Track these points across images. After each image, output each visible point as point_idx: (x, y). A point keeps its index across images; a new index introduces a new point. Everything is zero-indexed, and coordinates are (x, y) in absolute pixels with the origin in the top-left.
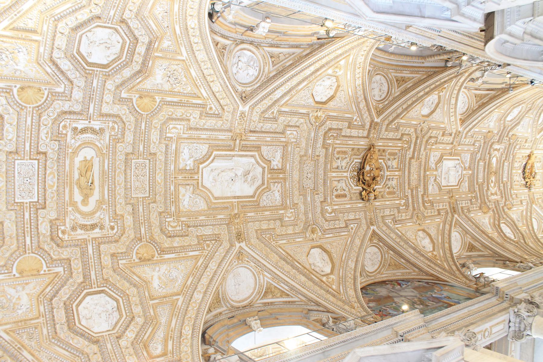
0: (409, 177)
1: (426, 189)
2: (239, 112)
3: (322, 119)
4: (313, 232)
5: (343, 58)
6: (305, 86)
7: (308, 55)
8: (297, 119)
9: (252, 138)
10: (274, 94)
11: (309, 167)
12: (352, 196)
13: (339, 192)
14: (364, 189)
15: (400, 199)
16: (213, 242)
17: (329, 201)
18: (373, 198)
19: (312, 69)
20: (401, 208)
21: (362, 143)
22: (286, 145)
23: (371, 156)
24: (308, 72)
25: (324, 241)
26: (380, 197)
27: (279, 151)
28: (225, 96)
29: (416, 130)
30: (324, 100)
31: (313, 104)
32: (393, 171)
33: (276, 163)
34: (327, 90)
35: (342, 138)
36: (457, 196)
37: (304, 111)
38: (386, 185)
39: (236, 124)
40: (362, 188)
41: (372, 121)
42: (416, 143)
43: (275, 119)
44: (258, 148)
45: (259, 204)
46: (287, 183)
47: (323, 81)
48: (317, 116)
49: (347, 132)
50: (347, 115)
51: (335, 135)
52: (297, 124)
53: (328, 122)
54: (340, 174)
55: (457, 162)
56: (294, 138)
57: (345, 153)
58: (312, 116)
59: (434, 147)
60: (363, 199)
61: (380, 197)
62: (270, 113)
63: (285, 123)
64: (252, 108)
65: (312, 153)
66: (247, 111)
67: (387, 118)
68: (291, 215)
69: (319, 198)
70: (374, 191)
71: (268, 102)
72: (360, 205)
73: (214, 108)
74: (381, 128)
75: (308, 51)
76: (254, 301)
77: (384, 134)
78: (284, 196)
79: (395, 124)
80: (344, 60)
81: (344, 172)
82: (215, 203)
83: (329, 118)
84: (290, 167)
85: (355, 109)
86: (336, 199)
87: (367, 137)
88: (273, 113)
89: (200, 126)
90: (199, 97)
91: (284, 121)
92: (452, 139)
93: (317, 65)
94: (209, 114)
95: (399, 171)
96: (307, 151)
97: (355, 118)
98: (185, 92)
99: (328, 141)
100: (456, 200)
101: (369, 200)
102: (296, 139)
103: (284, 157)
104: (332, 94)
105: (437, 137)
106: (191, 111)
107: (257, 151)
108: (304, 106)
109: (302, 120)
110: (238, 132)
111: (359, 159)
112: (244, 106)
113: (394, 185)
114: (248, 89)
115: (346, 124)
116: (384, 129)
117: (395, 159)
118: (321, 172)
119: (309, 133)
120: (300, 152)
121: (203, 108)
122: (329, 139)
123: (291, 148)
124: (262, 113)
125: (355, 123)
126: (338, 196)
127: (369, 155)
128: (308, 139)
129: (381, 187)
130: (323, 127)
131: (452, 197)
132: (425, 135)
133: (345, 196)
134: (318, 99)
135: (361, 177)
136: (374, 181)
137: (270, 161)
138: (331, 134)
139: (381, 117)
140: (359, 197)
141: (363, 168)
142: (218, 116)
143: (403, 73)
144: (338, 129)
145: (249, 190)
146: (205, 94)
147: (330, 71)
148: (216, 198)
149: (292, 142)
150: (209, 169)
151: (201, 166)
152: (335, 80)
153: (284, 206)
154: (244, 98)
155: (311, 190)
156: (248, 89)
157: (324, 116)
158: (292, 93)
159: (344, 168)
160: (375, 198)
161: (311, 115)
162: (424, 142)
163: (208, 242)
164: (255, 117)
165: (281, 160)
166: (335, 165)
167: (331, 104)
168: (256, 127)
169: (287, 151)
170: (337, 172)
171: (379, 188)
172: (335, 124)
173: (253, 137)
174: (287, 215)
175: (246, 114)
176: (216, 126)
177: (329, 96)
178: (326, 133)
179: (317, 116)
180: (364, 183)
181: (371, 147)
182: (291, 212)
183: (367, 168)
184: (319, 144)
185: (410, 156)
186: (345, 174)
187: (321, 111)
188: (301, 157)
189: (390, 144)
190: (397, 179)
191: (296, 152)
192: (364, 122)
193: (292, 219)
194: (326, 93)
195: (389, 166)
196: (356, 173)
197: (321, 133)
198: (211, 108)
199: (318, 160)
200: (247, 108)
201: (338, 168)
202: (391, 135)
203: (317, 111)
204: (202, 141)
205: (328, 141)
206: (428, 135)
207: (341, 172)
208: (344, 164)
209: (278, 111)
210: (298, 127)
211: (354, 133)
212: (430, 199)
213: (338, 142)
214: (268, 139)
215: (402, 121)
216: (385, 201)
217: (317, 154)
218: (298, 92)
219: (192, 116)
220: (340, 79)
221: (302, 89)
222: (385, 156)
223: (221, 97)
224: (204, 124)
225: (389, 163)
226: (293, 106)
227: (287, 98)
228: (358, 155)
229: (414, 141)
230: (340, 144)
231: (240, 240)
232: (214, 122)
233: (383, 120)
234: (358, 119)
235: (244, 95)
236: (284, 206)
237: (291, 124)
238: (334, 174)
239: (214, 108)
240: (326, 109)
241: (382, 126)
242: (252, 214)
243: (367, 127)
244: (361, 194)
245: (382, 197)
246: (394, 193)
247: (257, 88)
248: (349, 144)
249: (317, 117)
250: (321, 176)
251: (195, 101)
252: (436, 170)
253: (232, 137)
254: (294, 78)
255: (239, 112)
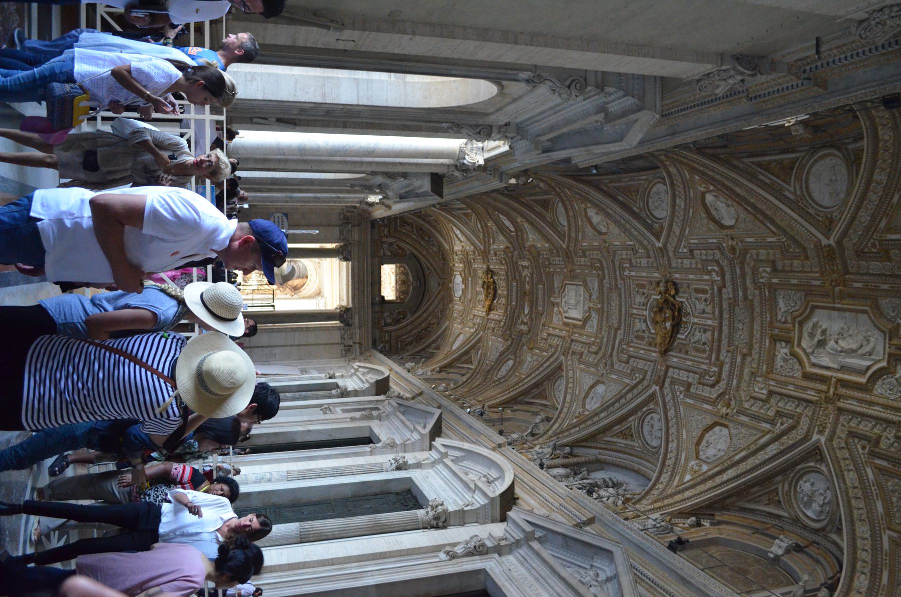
0: (620, 305)
1: (601, 285)
2: (826, 433)
3: (721, 403)
5: (685, 483)
6: (737, 454)
7: (728, 497)
8: (753, 408)
10: (779, 451)
11: (741, 337)
12: (687, 290)
13: (703, 297)
14: (674, 297)
15: (630, 277)
17: (715, 287)
18: (661, 284)
19: (725, 477)
20: (628, 265)
21: (675, 360)
22: (769, 373)
23: (665, 341)
24: (731, 473)
26: (654, 283)
27: (778, 366)
28: (842, 463)
29: (612, 366)
30: (717, 429)
31: (731, 425)
32: (639, 315)
33: (782, 351)
34: (712, 441)
35: (699, 371)
36: (565, 270)
37: (743, 418)
38: (648, 297)
39: (831, 416)
40: (675, 299)
41: (662, 387)
42: (613, 349)
43: (779, 414)
44: (807, 376)
46: (768, 319)
47: (715, 456)
48: (727, 408)
49: (692, 378)
50: (691, 402)
51: (707, 377)
52: (752, 401)
53: (714, 396)
54: (703, 321)
55: (567, 315)
56: (759, 382)
57: (697, 350)
58: (733, 409)
59: (593, 339)
60: (674, 284)
61: (654, 283)
62: (785, 425)
63: (768, 406)
64: (807, 438)
65: (736, 356)
66: (815, 434)
67: (646, 388)
69: (727, 293)
70: (660, 293)
71: (787, 441)
72: (677, 276)
73: (859, 447)
74: (651, 376)
75: (729, 501)
77: (649, 367)
78: (774, 306)
79: (636, 379)
80: (685, 481)
81: (697, 324)
83: (713, 403)
84: (765, 342)
85: (681, 408)
87: (668, 367)
88: (782, 424)
89: (882, 424)
90: (876, 468)
91: (769, 409)
92: (572, 346)
93: (718, 480)
94: (867, 440)
96: (743, 362)
97: (682, 396)
98: (897, 481)
99: (716, 369)
100: (566, 266)
101: (667, 282)
102: (755, 380)
104: (707, 435)
105: (589, 352)
106: (892, 449)
108: (742, 424)
109: (746, 405)
110: (830, 406)
111: (679, 338)
112: (818, 441)
113: (638, 296)
114: (812, 464)
115: (692, 390)
116: (649, 374)
117: (637, 331)
118: (725, 329)
119: (738, 386)
120: (752, 361)
121: (872, 451)
122: (714, 371)
123: (762, 369)
125: (682, 389)
126: (704, 291)
127: (667, 342)
128: (740, 377)
129: (653, 297)
130: (721, 391)
131: (570, 271)
132: (602, 358)
133: (697, 291)
134: (725, 431)
135: (676, 314)
136: (661, 306)
138: (713, 379)
139: (651, 391)
140: (679, 286)
141: (673, 327)
142: (852, 434)
144: (704, 384)
146: (869, 470)
147: (705, 468)
149: (760, 376)
152: (701, 453)
154: (816, 453)
155: (738, 306)
156: (812, 464)
157: (719, 406)
158: (753, 448)
159: (697, 330)
160: (658, 283)
161: (735, 411)
162: (603, 348)
164: (804, 423)
165: (777, 353)
166: (709, 334)
167: (709, 421)
168: (805, 408)
169: (768, 364)
170: (706, 325)
171: (655, 295)
172: (706, 393)
173: (811, 395)
175: (816, 430)
176: (859, 419)
177: (711, 433)
178: (717, 382)
179: (727, 408)
180: (673, 305)
181: (665, 353)
183: (668, 325)
184: (726, 368)
185: (619, 332)
186: (696, 320)
187: (721, 413)
188: (750, 354)
189: (642, 352)
190: (635, 304)
191: (756, 361)
192: (671, 388)
194: (713, 437)
195: (644, 322)
196: (684, 319)
197: (723, 384)
198: (863, 448)
199: (729, 346)
201: (705, 331)
202: (641, 364)
203: (727, 414)
204: (881, 401)
205: (716, 369)
206: (598, 357)
207: (702, 324)
208: (698, 335)
209: (775, 425)
210: (751, 397)
211: (683, 376)
212: (595, 272)
213: (704, 367)
214: (791, 387)
216: (647, 277)
217: (730, 354)
218: (748, 447)
219: (891, 442)
220: (694, 455)
221: (742, 451)
222: (648, 337)
223: (847, 462)
224: (875, 426)
225: (644, 327)
226: (755, 429)
227: (762, 441)
228: (681, 344)
229: (615, 351)
230: (703, 363)
232: (861, 427)
233: (648, 387)
234: (678, 393)
235: (818, 457)
237: (761, 404)
238: (710, 322)
239: (859, 447)
240: (715, 415)
241: (651, 380)
243: (668, 380)
244: (677, 291)
245: (651, 282)
246: (637, 285)
247: (800, 463)
248: (693, 361)
249: (728, 405)
250: (725, 322)
251: (885, 463)
252: (590, 308)
253: (839, 400)
254: (749, 468)
255: (826, 433)
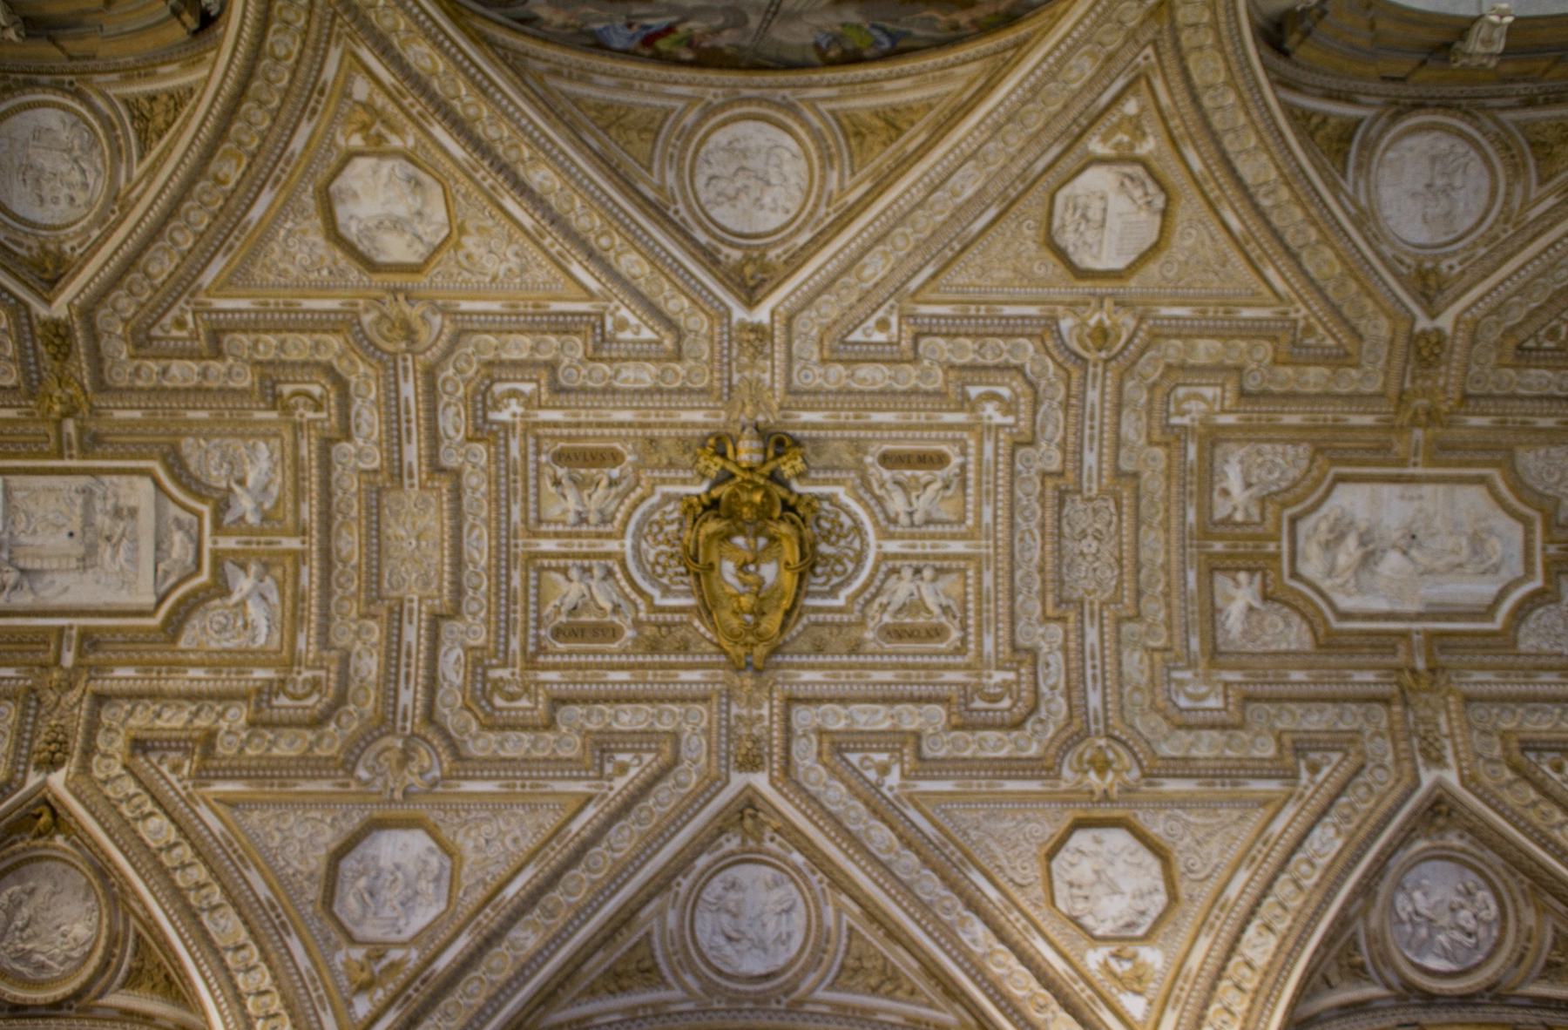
4: (1103, 335)
9: (1369, 677)
16: (1531, 343)
25: (1055, 293)
45: (1318, 450)
68: (1186, 406)
76: (1384, 119)
82: (1486, 464)
86: (944, 448)
95: (533, 556)
103: (1212, 614)
107: (1330, 633)
124: (1363, 766)
137: (1266, 597)
143: (624, 1011)
145: (1351, 500)
148: (1481, 480)
150: (1506, 575)
151: (1537, 583)
153: (1213, 438)
163: (1548, 344)
174: (1203, 406)
182: (1182, 414)
193: (1181, 391)
200: (1428, 778)
215: (580, 787)
231: (1433, 339)
236: (1213, 438)
242: (1356, 420)
